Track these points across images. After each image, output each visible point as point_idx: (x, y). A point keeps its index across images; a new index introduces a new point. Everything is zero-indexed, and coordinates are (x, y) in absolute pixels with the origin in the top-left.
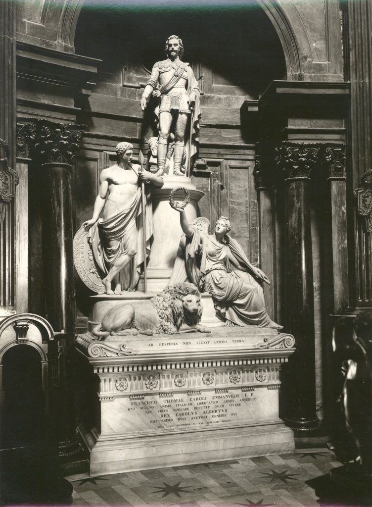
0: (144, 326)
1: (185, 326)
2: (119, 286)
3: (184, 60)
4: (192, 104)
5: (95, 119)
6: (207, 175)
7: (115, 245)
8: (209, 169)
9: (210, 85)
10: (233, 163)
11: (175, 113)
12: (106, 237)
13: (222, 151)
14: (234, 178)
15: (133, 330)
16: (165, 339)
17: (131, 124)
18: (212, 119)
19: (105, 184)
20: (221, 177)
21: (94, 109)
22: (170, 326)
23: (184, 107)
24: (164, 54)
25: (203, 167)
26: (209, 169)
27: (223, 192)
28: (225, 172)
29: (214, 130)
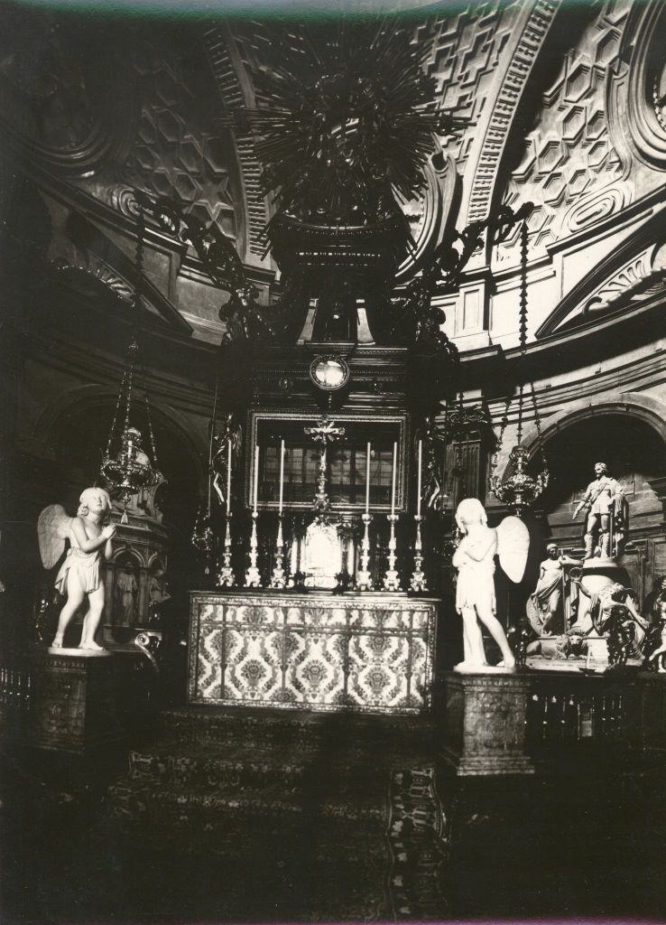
0: (547, 654)
1: (572, 655)
2: (550, 632)
3: (608, 476)
4: (611, 507)
5: (553, 530)
6: (636, 553)
7: (545, 607)
8: (637, 548)
9: (640, 485)
10: (658, 540)
11: (598, 516)
12: (543, 600)
13: (647, 533)
14: (660, 552)
15: (540, 656)
16: (557, 662)
17: (578, 527)
18: (641, 509)
19: (542, 571)
20: (646, 553)
21: (551, 524)
22: (563, 655)
23: (605, 510)
24: (593, 477)
25: (632, 547)
26: (637, 548)
27: (648, 563)
28: (650, 548)
29: (642, 518)
